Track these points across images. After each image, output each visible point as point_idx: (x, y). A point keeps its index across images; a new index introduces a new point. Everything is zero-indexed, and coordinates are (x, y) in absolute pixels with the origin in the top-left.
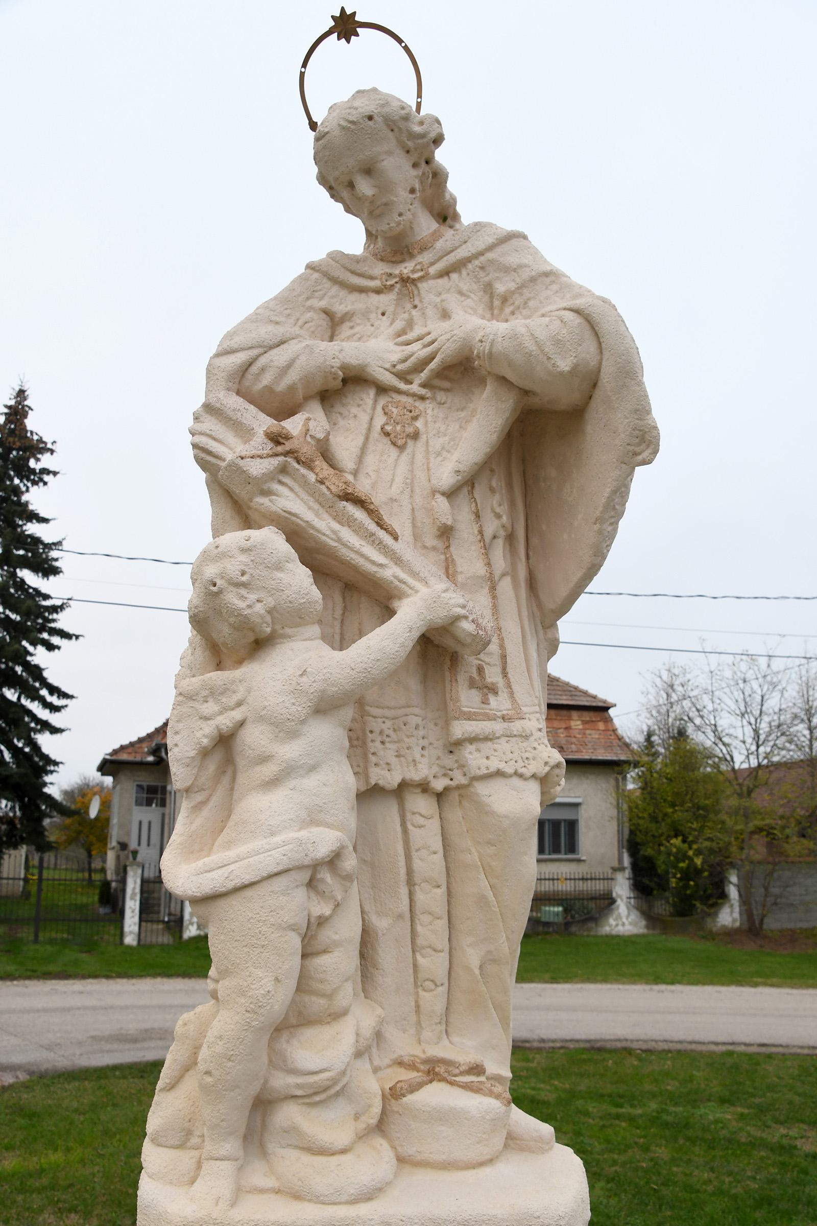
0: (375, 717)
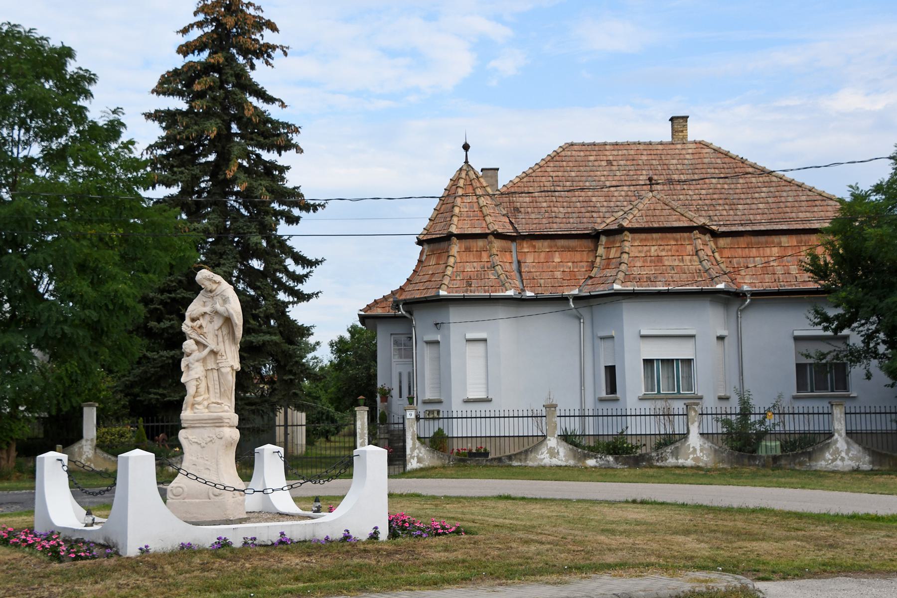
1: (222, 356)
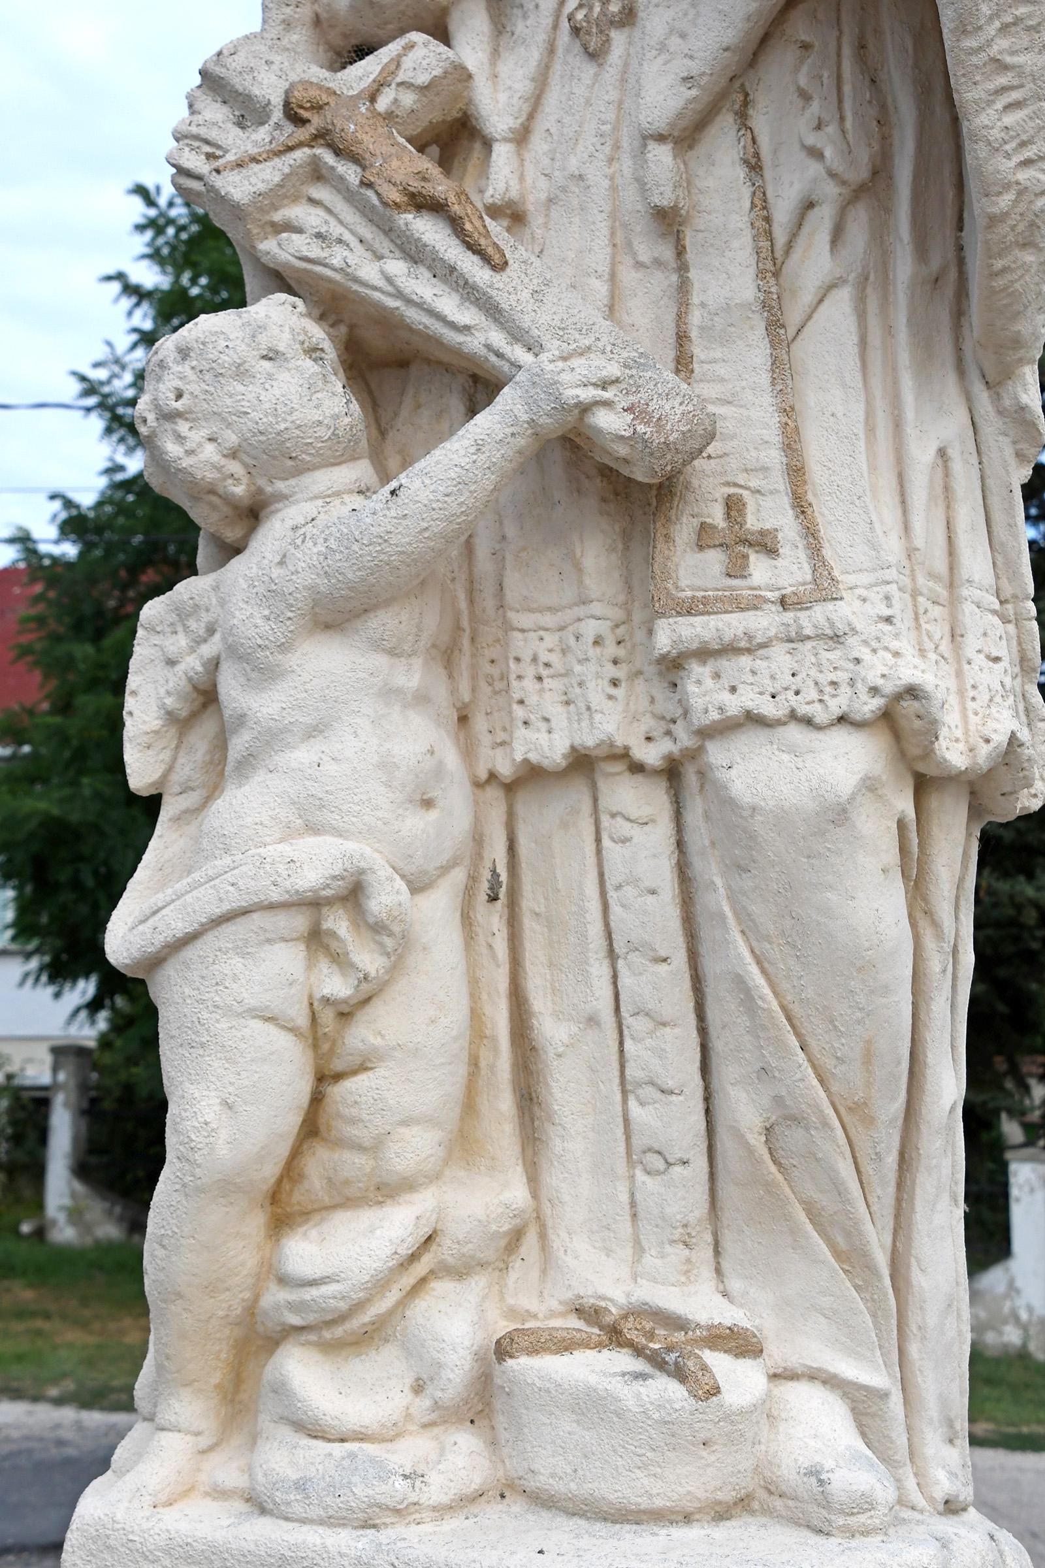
0: (523, 631)
1: (743, 543)
